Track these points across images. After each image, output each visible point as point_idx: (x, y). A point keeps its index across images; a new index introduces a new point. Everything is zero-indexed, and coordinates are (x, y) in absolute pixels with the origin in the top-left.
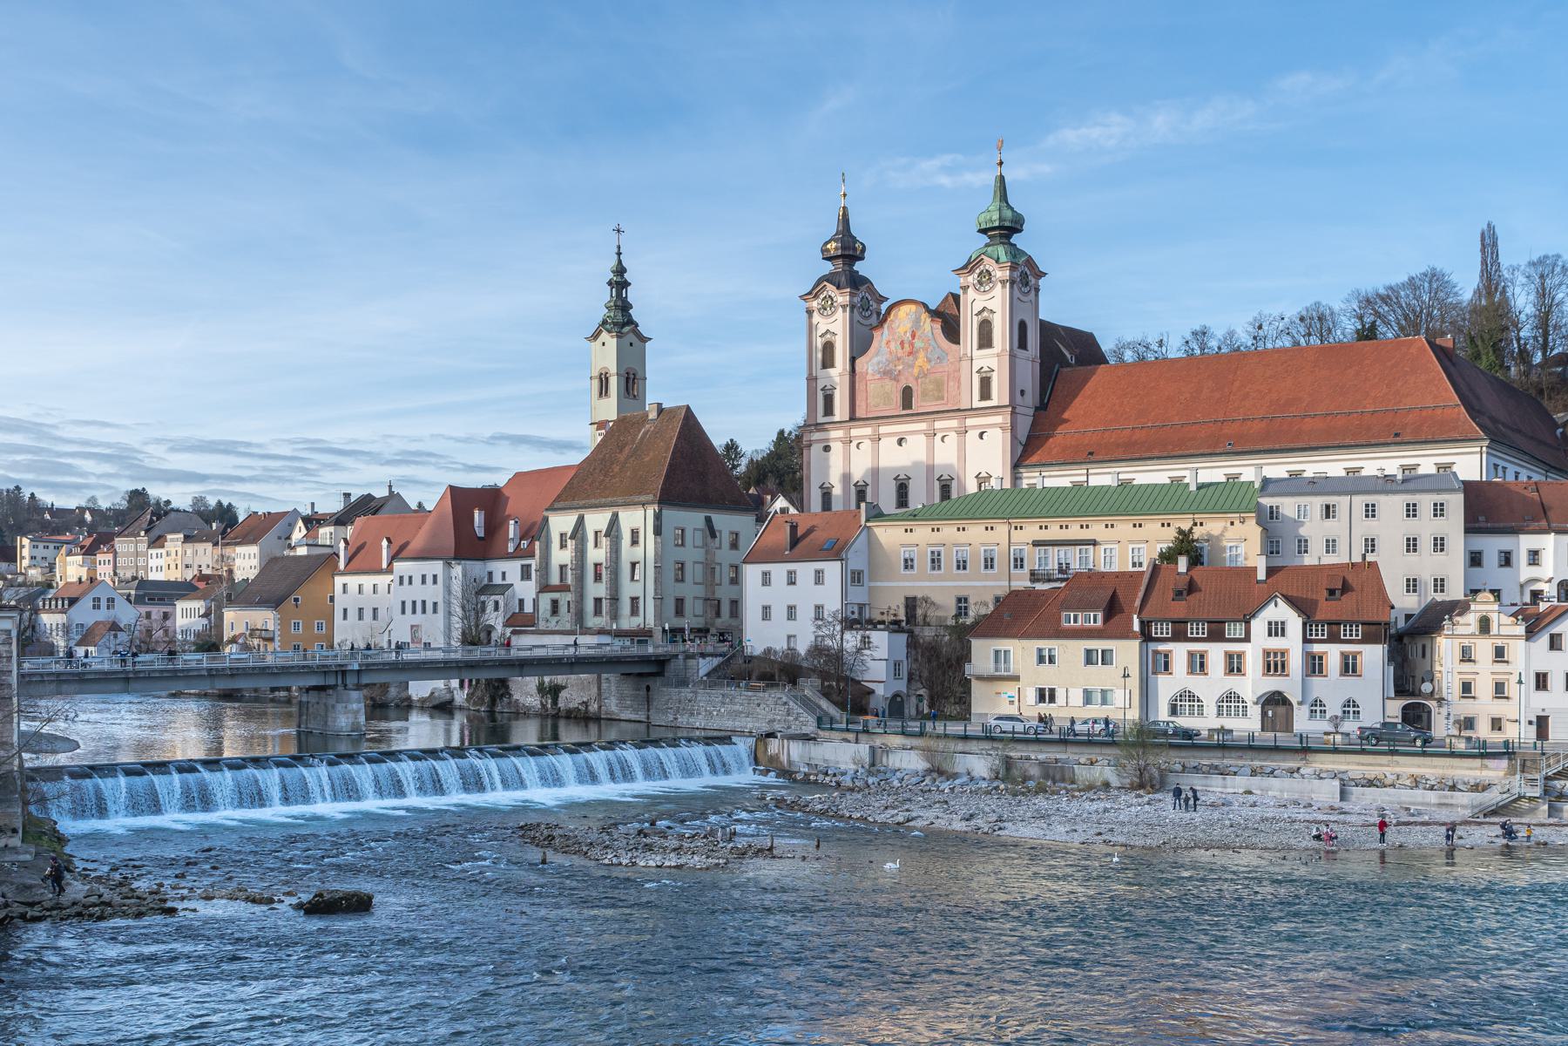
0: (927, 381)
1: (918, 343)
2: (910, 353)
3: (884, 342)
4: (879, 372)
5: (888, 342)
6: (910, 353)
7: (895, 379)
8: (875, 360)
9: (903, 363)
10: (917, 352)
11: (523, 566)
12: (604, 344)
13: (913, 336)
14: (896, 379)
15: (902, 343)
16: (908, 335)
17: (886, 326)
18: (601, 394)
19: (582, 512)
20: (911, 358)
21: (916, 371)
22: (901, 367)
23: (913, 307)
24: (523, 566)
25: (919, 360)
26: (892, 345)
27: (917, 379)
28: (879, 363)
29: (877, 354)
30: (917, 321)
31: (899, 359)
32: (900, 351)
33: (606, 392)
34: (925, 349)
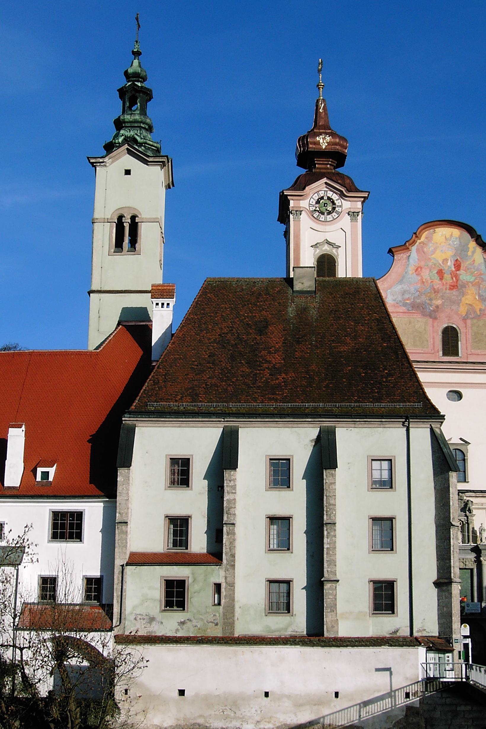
0: (481, 323)
1: (464, 276)
2: (453, 287)
3: (411, 269)
4: (405, 305)
5: (418, 270)
6: (453, 287)
7: (431, 317)
8: (398, 288)
9: (442, 297)
10: (464, 286)
11: (56, 515)
12: (128, 172)
13: (458, 266)
14: (433, 315)
15: (441, 273)
16: (450, 264)
17: (414, 248)
18: (119, 244)
19: (232, 423)
20: (455, 292)
21: (463, 310)
22: (439, 302)
23: (456, 232)
24: (56, 515)
25: (468, 297)
26: (426, 274)
27: (465, 320)
28: (404, 293)
29: (401, 281)
30: (463, 249)
31: (436, 291)
32: (436, 278)
33: (134, 242)
34: (477, 285)
